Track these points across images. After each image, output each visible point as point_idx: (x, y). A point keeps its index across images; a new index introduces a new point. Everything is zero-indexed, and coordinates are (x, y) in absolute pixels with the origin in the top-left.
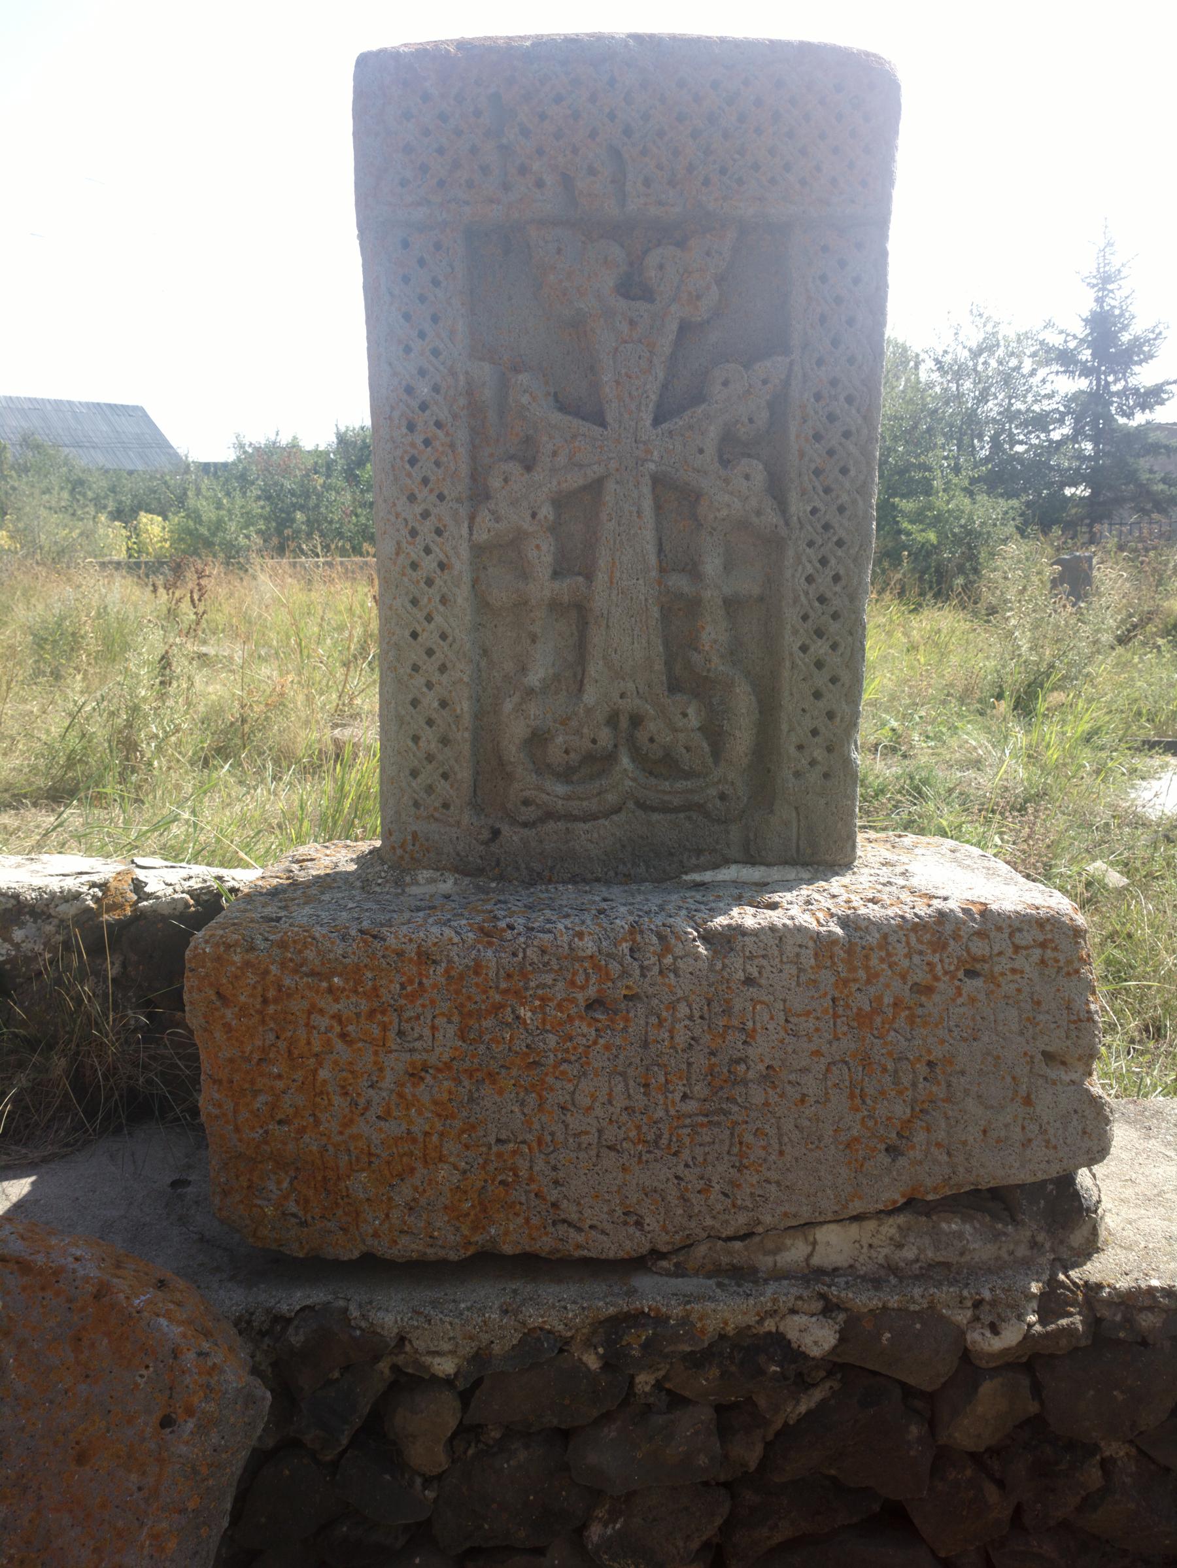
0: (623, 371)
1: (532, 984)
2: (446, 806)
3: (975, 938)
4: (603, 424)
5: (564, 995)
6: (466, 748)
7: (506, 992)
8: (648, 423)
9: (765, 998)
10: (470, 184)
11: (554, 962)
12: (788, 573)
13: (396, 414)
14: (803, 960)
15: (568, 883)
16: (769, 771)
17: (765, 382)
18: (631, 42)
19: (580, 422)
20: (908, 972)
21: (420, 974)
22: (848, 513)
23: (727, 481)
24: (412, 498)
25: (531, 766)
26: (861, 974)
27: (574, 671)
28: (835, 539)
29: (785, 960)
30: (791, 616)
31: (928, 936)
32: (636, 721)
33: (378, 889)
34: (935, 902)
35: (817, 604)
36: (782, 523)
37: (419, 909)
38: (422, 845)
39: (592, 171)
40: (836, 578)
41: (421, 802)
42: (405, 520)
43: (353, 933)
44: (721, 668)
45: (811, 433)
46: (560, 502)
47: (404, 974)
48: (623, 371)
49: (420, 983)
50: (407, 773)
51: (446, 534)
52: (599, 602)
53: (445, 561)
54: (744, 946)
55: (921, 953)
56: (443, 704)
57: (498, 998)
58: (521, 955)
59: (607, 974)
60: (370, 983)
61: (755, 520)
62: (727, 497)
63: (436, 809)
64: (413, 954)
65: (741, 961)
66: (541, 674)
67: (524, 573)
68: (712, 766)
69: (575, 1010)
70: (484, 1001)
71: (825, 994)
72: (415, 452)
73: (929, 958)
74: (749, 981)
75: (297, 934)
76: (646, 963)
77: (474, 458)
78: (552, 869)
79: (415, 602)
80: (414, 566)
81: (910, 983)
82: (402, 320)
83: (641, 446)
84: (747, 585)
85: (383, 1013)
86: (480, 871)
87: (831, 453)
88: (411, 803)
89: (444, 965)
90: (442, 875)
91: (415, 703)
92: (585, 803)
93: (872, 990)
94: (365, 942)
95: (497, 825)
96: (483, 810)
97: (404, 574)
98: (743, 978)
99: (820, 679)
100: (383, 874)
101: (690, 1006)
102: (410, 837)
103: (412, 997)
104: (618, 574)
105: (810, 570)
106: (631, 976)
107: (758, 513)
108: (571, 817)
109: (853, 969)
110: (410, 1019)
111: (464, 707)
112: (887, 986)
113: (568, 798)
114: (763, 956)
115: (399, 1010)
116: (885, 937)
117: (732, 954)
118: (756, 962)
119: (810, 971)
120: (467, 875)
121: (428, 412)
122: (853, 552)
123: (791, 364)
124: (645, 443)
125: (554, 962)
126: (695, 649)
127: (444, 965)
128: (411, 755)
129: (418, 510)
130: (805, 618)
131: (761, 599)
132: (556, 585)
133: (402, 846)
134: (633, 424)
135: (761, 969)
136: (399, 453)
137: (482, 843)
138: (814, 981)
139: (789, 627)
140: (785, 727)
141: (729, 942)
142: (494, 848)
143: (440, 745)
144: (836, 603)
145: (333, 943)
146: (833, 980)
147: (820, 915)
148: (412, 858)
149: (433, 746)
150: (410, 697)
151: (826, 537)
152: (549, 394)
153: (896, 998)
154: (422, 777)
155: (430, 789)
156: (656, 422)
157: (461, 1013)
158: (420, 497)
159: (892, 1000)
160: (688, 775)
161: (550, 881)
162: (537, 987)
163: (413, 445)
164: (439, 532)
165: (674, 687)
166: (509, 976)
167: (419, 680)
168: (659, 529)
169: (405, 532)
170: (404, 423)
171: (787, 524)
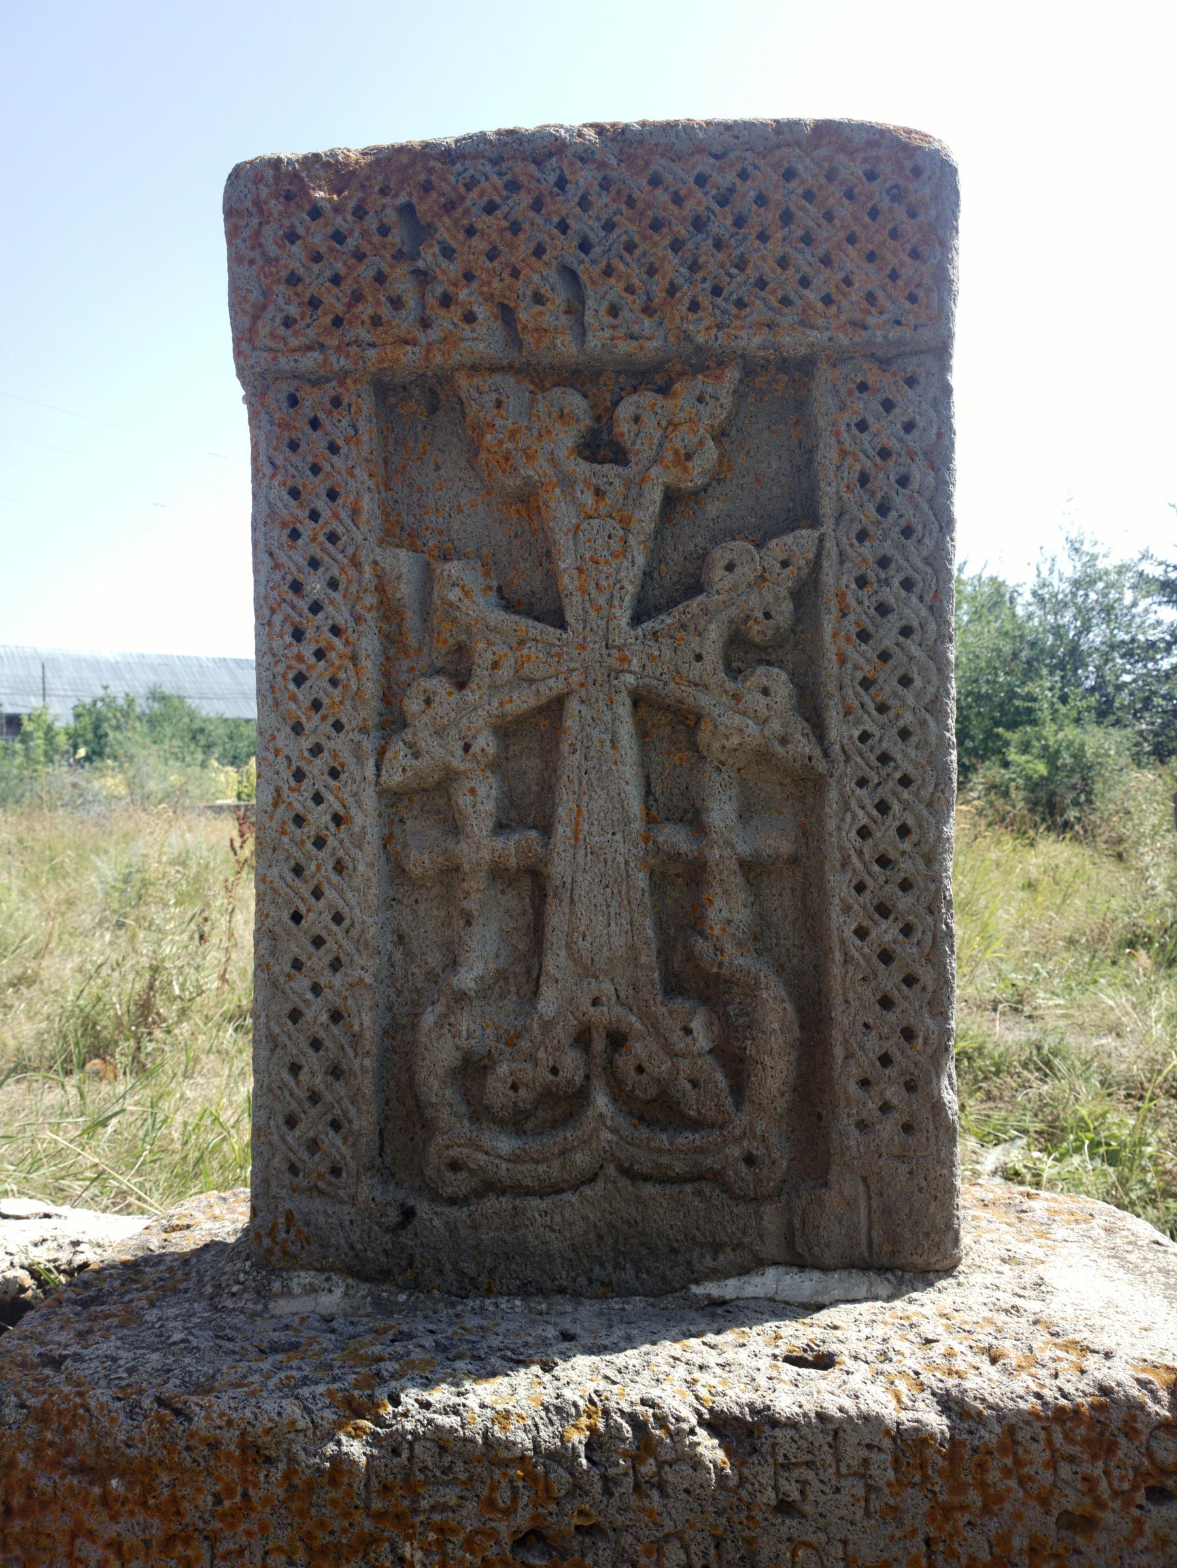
0: (588, 555)
1: (424, 1504)
2: (336, 1171)
3: (1161, 1434)
4: (562, 625)
5: (476, 1524)
6: (367, 1086)
7: (379, 1516)
8: (624, 621)
9: (811, 1538)
10: (376, 321)
11: (459, 1467)
12: (832, 824)
13: (278, 618)
14: (874, 1471)
15: (516, 1295)
16: (820, 1118)
17: (785, 564)
18: (591, 134)
19: (531, 622)
20: (1051, 1493)
21: (245, 1480)
22: (914, 739)
23: (737, 697)
24: (298, 729)
25: (463, 1109)
26: (974, 1497)
27: (526, 971)
28: (898, 775)
29: (844, 1471)
30: (839, 884)
31: (1083, 1430)
32: (617, 1040)
33: (229, 1304)
34: (1091, 1362)
35: (876, 868)
36: (817, 753)
37: (275, 1349)
38: (299, 1232)
39: (539, 299)
40: (903, 831)
41: (300, 1165)
42: (288, 757)
43: (147, 1403)
44: (740, 961)
45: (854, 630)
46: (505, 730)
47: (219, 1479)
48: (588, 555)
49: (245, 1495)
50: (281, 1121)
51: (343, 777)
52: (560, 868)
53: (342, 813)
54: (774, 1445)
55: (1072, 1459)
56: (336, 1017)
57: (368, 1525)
58: (405, 1454)
59: (548, 1489)
60: (166, 1492)
61: (779, 749)
62: (737, 719)
63: (320, 1176)
64: (233, 1447)
65: (770, 1471)
66: (478, 969)
67: (454, 828)
68: (731, 1109)
69: (495, 1550)
70: (344, 1531)
71: (914, 1532)
72: (303, 667)
73: (1086, 1468)
74: (785, 1507)
75: (67, 1398)
76: (612, 1471)
77: (387, 675)
78: (492, 1271)
79: (298, 870)
80: (299, 820)
81: (1056, 1513)
82: (286, 497)
83: (614, 652)
84: (776, 841)
85: (187, 1542)
86: (383, 1275)
87: (884, 656)
88: (285, 1167)
89: (282, 1466)
90: (328, 1279)
91: (295, 1015)
92: (542, 1168)
93: (993, 1524)
94: (160, 1420)
95: (411, 1202)
96: (393, 1175)
97: (283, 833)
98: (774, 1503)
99: (889, 979)
100: (242, 1277)
101: (685, 1548)
102: (282, 1220)
103: (231, 1519)
104: (586, 827)
105: (863, 819)
106: (587, 1493)
107: (784, 741)
108: (522, 1191)
109: (958, 1488)
110: (230, 1553)
111: (366, 1020)
112: (1018, 1517)
113: (515, 1159)
114: (809, 1464)
115: (212, 1539)
116: (1011, 1430)
117: (755, 1459)
118: (795, 1473)
119: (887, 1491)
120: (366, 1280)
121: (320, 615)
122: (925, 793)
123: (821, 539)
124: (620, 649)
125: (459, 1467)
126: (701, 933)
127: (282, 1466)
128: (287, 1094)
129: (306, 743)
130: (860, 888)
131: (794, 860)
132: (499, 843)
133: (271, 1233)
134: (603, 623)
135: (804, 1484)
136: (280, 668)
137: (387, 1231)
138: (895, 1509)
139: (836, 901)
140: (839, 1052)
141: (751, 1434)
142: (405, 1238)
143: (329, 1078)
144: (906, 867)
145: (113, 1420)
146: (925, 1507)
147: (902, 1386)
148: (285, 1253)
149: (319, 1079)
150: (289, 1007)
151: (883, 773)
152: (490, 588)
153: (1034, 1539)
154: (302, 1126)
155: (313, 1146)
156: (637, 619)
157: (309, 1550)
158: (308, 726)
159: (1026, 1542)
160: (696, 1125)
161: (489, 1292)
162: (433, 1508)
163: (300, 658)
164: (334, 774)
165: (673, 987)
166: (386, 1489)
167: (302, 983)
168: (644, 764)
169: (287, 774)
170: (289, 629)
171: (826, 754)
